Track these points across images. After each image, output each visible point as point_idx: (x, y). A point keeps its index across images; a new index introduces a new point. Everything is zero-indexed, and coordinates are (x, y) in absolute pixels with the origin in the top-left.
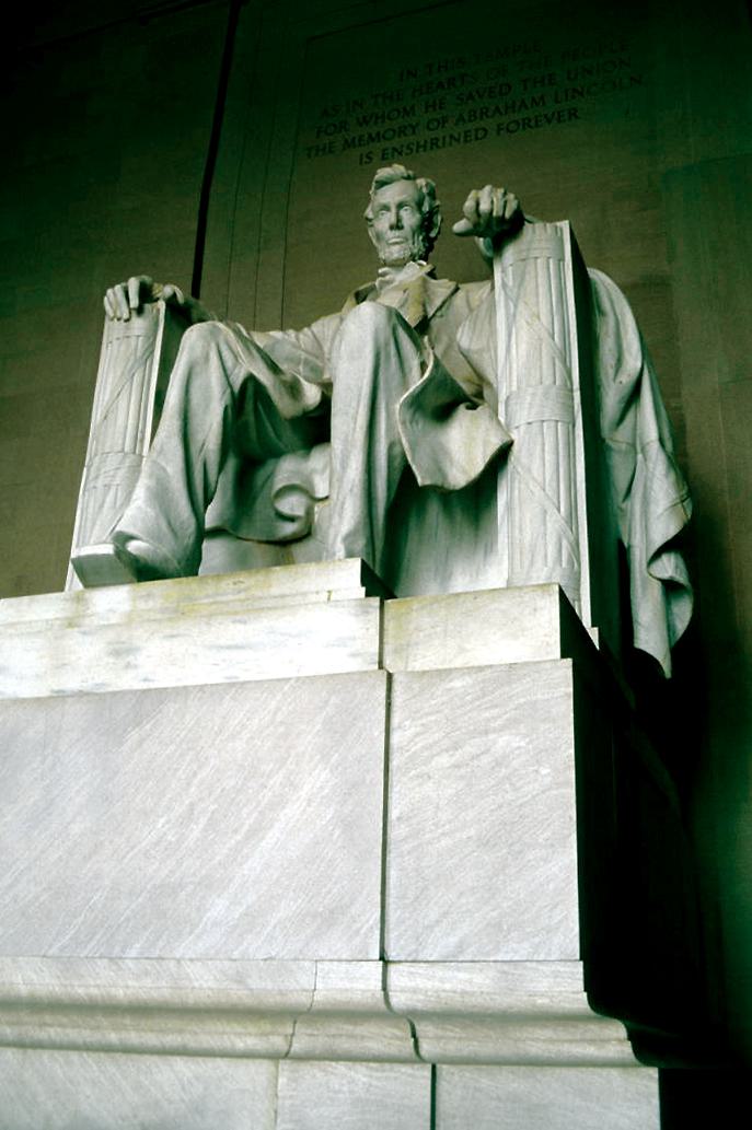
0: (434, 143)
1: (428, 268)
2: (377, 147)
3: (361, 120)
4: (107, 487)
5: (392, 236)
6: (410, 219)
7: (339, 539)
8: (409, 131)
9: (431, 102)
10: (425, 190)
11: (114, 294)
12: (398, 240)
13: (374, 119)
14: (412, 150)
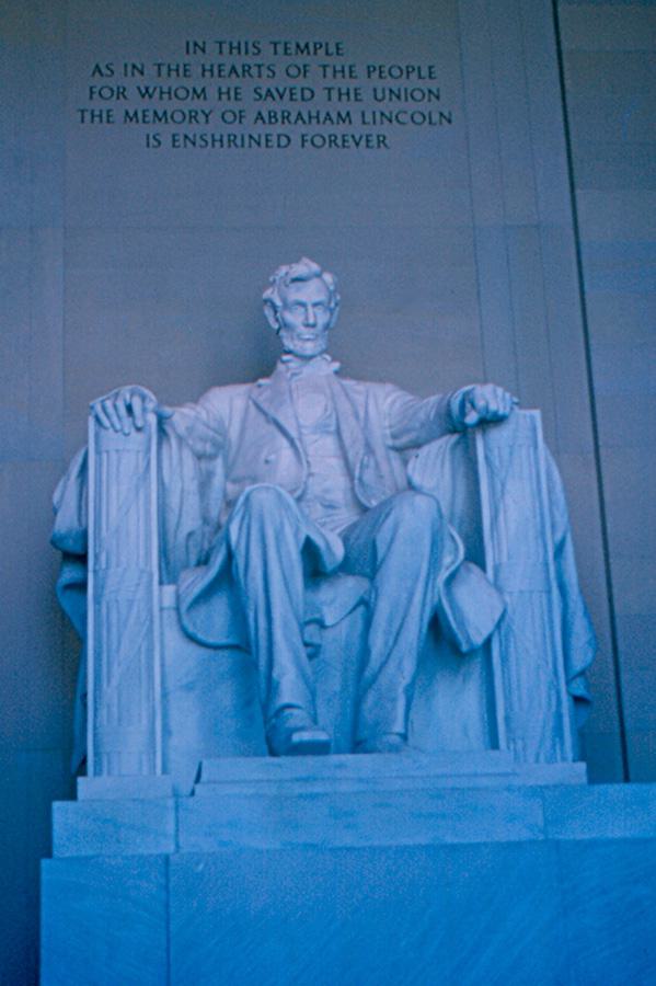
0: (232, 140)
1: (336, 366)
2: (165, 130)
3: (144, 91)
4: (131, 603)
5: (307, 333)
6: (322, 318)
7: (400, 690)
8: (201, 118)
9: (224, 90)
10: (332, 288)
11: (115, 407)
12: (312, 337)
13: (158, 90)
14: (206, 142)
